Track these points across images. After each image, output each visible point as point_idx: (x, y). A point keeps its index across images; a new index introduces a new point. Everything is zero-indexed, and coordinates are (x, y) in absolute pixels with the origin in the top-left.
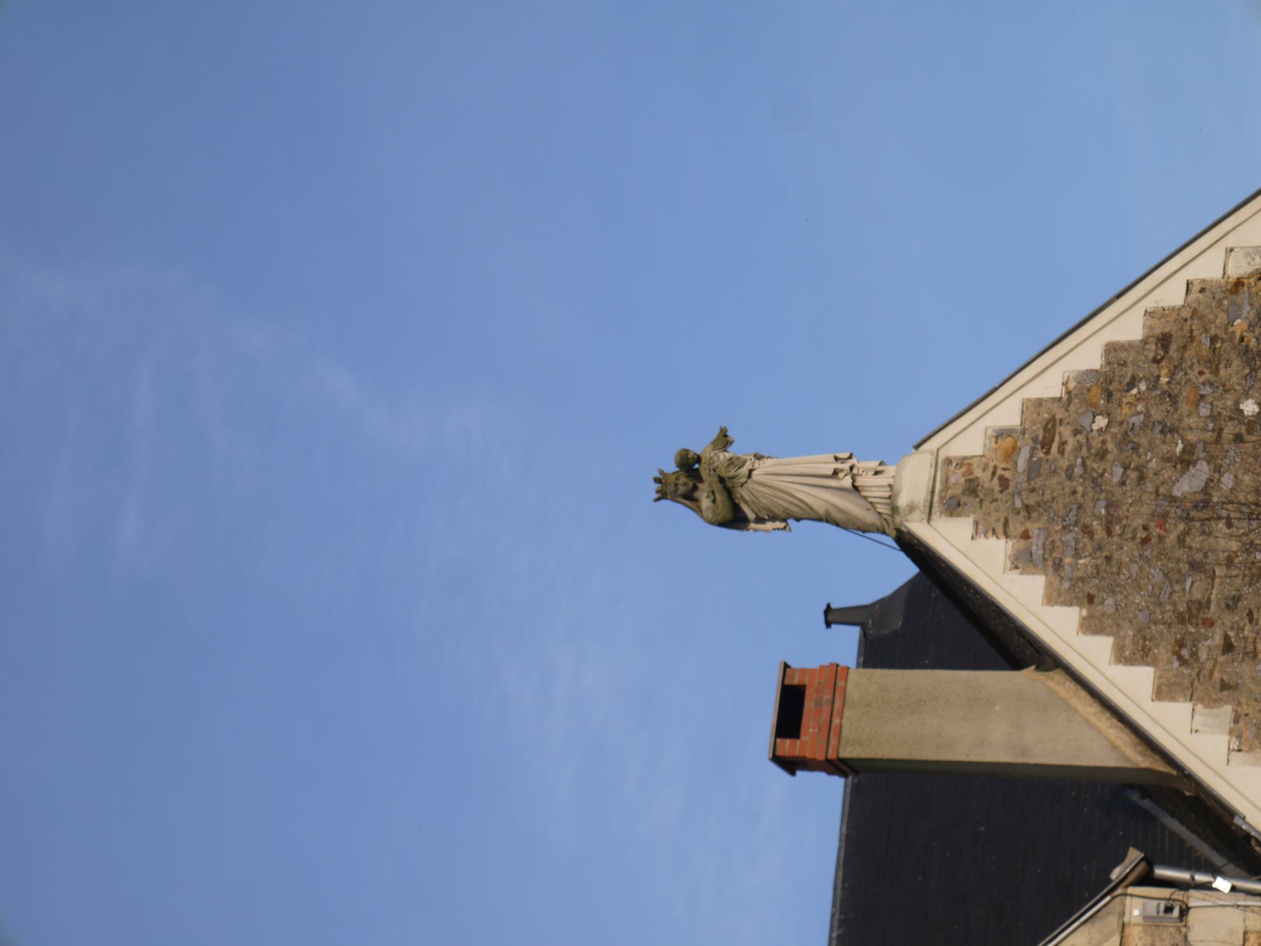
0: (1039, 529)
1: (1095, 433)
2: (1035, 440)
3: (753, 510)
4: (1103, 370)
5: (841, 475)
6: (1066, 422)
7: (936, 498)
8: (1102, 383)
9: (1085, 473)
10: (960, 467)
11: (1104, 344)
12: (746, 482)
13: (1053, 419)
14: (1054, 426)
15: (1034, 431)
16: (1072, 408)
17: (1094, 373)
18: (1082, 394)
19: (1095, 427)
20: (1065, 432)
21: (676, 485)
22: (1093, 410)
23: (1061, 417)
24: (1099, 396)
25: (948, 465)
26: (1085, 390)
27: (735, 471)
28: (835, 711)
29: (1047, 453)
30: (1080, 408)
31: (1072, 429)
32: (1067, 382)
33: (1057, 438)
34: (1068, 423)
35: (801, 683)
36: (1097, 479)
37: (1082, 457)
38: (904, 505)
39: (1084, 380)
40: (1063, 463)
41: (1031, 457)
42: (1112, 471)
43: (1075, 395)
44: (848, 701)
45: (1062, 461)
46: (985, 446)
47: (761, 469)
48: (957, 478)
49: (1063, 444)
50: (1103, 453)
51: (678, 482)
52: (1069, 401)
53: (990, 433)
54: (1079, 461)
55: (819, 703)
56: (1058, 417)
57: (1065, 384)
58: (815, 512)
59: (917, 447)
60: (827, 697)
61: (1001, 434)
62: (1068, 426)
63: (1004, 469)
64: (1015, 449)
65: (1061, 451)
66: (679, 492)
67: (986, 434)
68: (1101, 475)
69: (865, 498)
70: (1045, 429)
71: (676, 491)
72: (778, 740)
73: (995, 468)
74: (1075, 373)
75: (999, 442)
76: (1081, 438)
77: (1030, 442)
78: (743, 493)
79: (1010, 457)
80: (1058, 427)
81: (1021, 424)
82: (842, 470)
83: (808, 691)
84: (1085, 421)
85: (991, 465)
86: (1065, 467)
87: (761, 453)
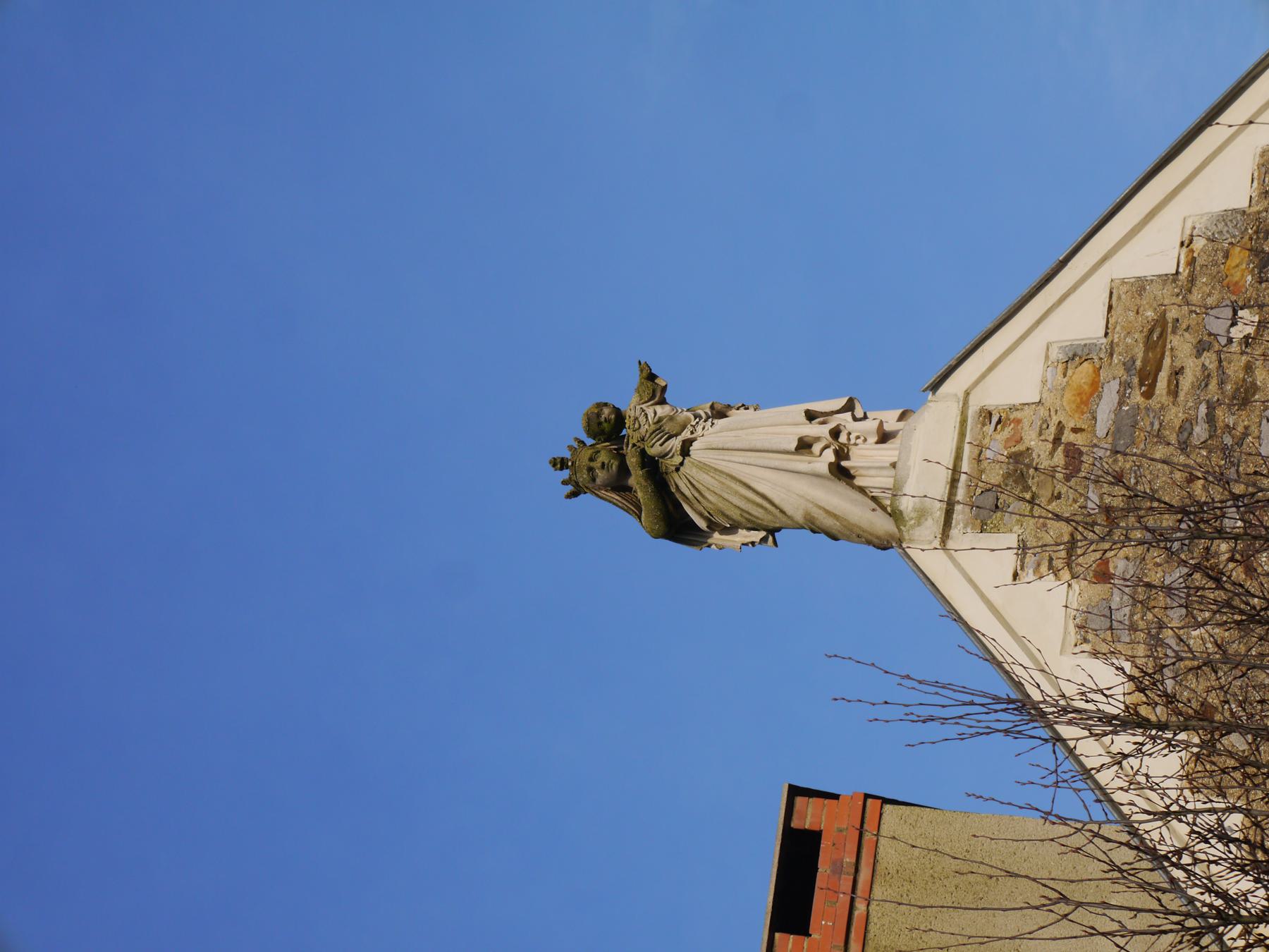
0: (1127, 558)
1: (1235, 347)
2: (1128, 366)
3: (701, 515)
4: (1255, 209)
5: (817, 448)
6: (1184, 326)
7: (961, 494)
8: (1251, 239)
9: (1211, 437)
10: (1003, 429)
11: (1259, 150)
12: (682, 464)
13: (1161, 321)
14: (1162, 335)
15: (1128, 348)
16: (1196, 297)
17: (1239, 217)
18: (1215, 264)
19: (1237, 333)
20: (1181, 346)
21: (591, 469)
22: (1234, 298)
23: (1176, 316)
24: (1244, 266)
25: (984, 425)
26: (1220, 255)
27: (661, 445)
28: (859, 892)
29: (1148, 395)
30: (1209, 295)
31: (1194, 342)
32: (1191, 242)
33: (1167, 362)
34: (1187, 330)
35: (816, 828)
36: (1232, 449)
37: (1208, 402)
38: (910, 508)
39: (1221, 232)
40: (1175, 416)
41: (1121, 403)
42: (1260, 432)
43: (1202, 266)
44: (880, 868)
45: (1174, 410)
46: (1044, 382)
47: (709, 437)
48: (998, 445)
49: (1177, 372)
50: (1246, 391)
51: (592, 464)
52: (1192, 279)
53: (1055, 354)
54: (1203, 409)
55: (838, 869)
56: (1172, 314)
57: (1186, 244)
58: (789, 517)
59: (935, 387)
60: (849, 859)
61: (1075, 356)
62: (1186, 335)
63: (1075, 430)
64: (1096, 386)
65: (1174, 392)
66: (598, 481)
67: (1047, 357)
68: (1240, 442)
69: (862, 490)
70: (1149, 345)
71: (594, 480)
72: (777, 935)
73: (1061, 427)
74: (1205, 218)
75: (1070, 372)
76: (1209, 359)
77: (1121, 372)
78: (680, 483)
79: (1086, 403)
80: (1170, 337)
81: (1106, 334)
82: (818, 439)
83: (824, 844)
84: (1218, 326)
85: (1055, 420)
86: (1177, 423)
87: (721, 401)
